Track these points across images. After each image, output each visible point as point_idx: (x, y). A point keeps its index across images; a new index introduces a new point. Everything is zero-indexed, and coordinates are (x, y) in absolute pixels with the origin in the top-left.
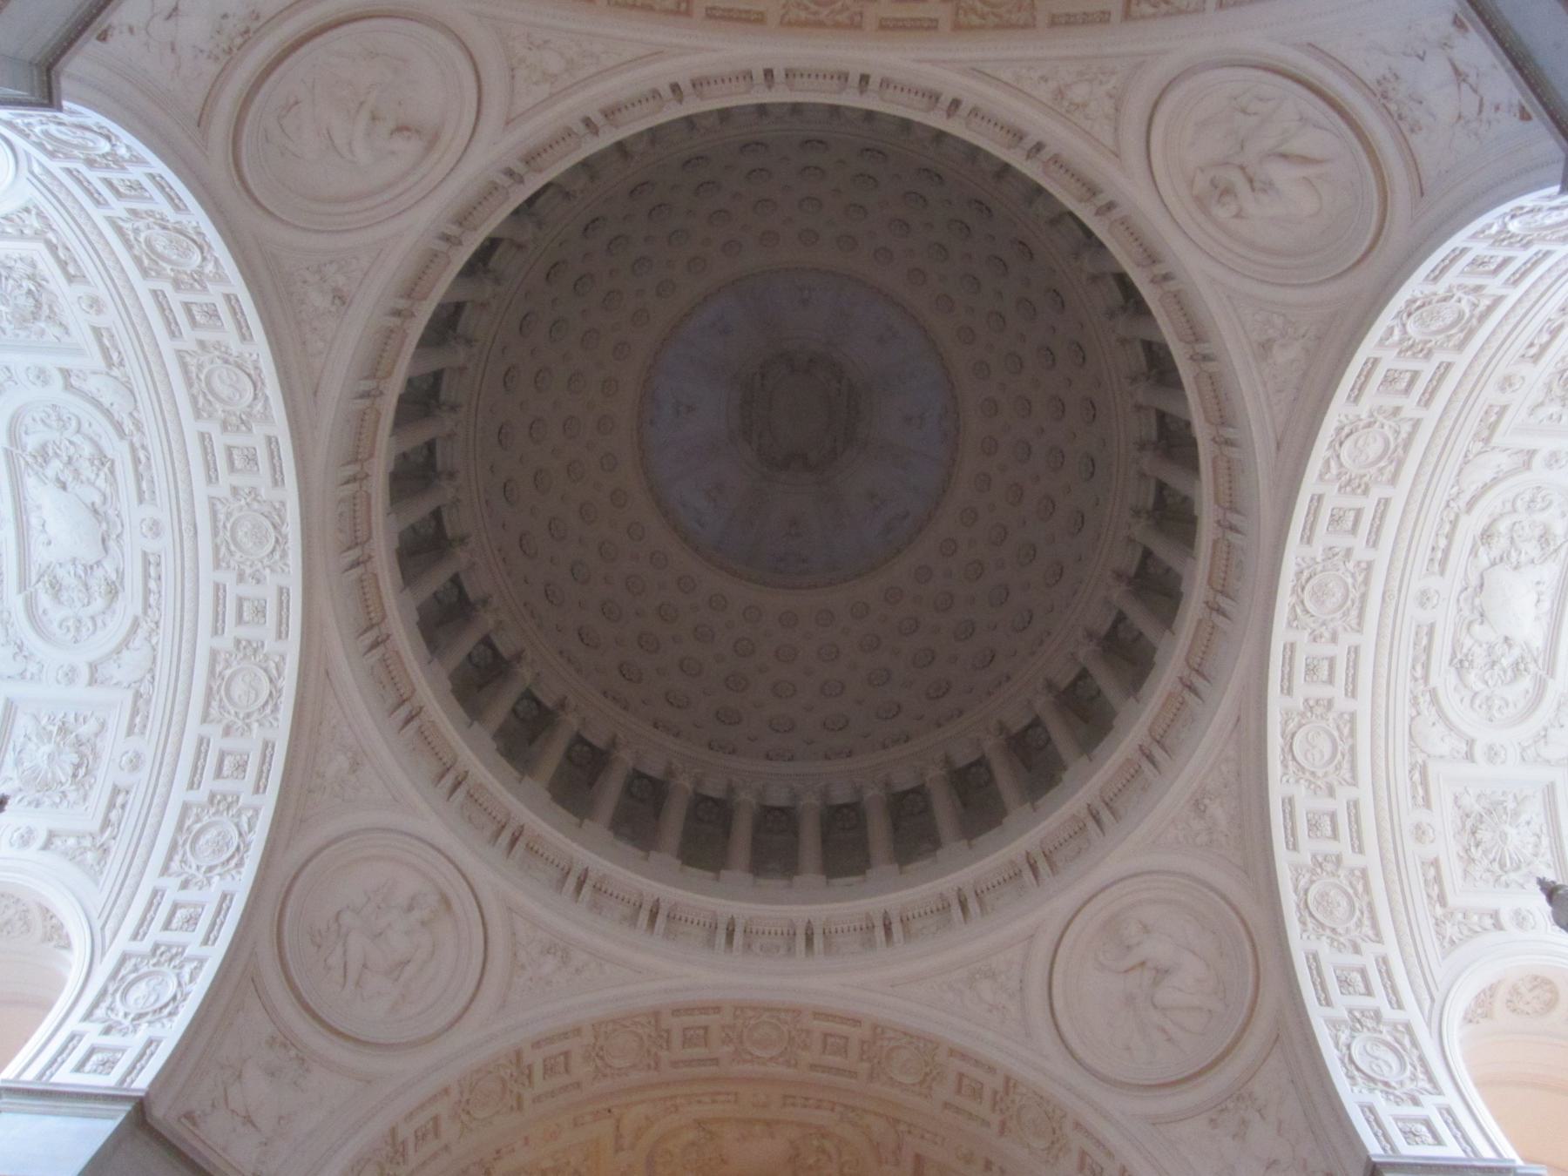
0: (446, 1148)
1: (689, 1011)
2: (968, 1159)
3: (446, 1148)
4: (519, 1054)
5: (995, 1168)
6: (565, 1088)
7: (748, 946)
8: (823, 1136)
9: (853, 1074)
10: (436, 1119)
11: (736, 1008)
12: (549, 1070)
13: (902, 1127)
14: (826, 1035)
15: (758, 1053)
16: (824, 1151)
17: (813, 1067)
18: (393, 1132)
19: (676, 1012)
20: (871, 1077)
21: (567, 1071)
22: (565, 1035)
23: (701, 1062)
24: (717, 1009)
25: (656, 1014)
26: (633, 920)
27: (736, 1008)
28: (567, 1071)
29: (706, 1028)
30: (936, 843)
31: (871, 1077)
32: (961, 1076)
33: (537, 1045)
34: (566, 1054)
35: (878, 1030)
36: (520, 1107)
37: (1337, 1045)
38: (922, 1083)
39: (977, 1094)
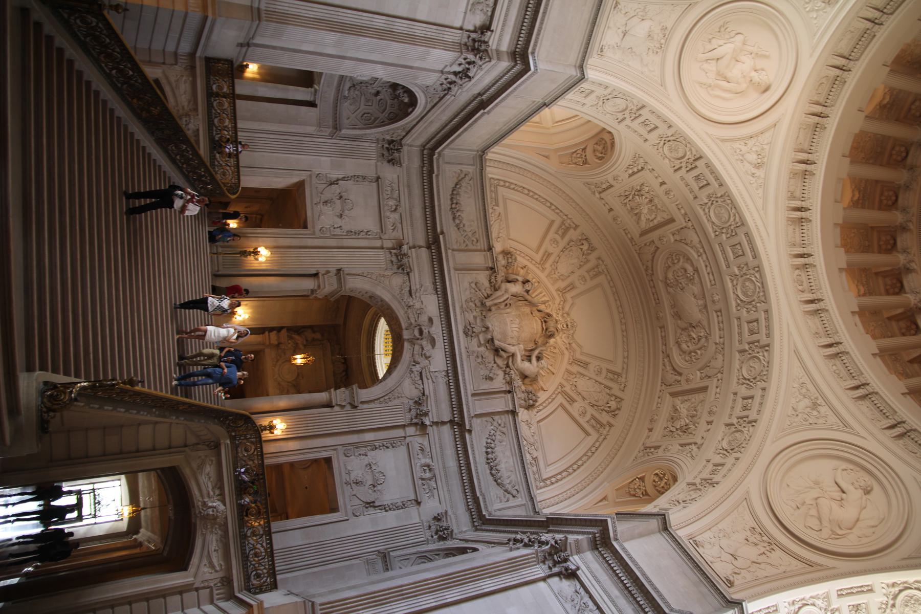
0: (646, 140)
1: (751, 242)
2: (711, 413)
3: (646, 140)
4: (701, 157)
5: (709, 426)
6: (692, 191)
7: (797, 268)
8: (706, 337)
9: (740, 342)
10: (656, 127)
11: (758, 267)
12: (697, 178)
13: (719, 375)
14: (757, 320)
15: (739, 288)
16: (699, 340)
17: (739, 319)
18: (643, 107)
19: (747, 235)
20: (742, 351)
21: (701, 188)
22: (717, 179)
23: (726, 259)
24: (755, 257)
25: (743, 224)
26: (792, 197)
27: (758, 267)
28: (701, 188)
29: (744, 255)
30: (874, 337)
31: (742, 351)
32: (752, 397)
33: (708, 165)
34: (708, 184)
35: (767, 347)
36: (675, 171)
37: (812, 597)
38: (745, 379)
39: (745, 408)
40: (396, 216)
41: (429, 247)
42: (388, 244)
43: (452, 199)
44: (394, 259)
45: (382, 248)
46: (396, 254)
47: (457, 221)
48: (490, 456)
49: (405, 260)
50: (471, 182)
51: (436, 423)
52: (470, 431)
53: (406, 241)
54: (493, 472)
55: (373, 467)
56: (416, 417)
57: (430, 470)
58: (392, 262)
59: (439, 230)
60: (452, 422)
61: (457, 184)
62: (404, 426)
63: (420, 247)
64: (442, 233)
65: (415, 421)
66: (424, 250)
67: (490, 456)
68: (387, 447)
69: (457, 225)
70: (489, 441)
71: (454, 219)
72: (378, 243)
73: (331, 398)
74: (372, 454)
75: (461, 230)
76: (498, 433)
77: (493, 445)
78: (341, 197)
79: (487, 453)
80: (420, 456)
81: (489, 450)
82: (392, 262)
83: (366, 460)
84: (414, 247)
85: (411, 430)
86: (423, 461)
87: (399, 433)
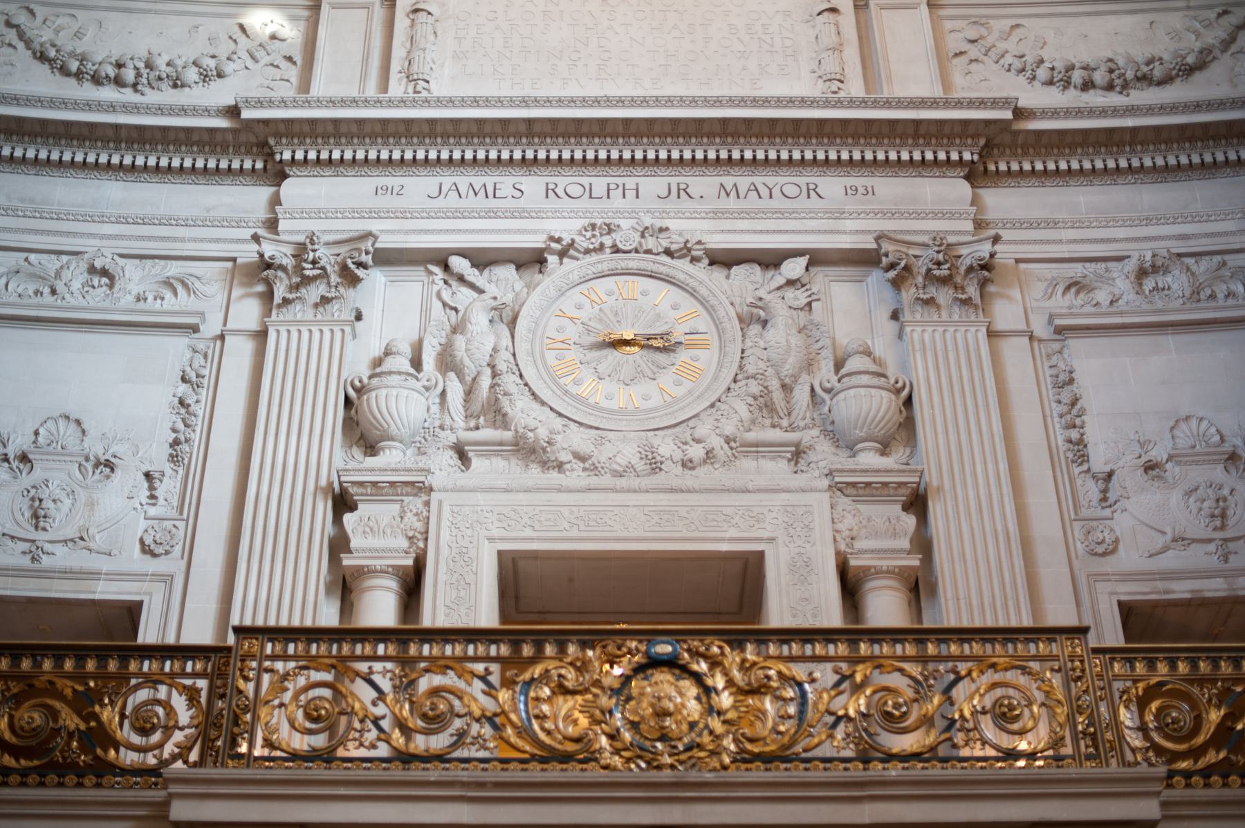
40: (134, 278)
41: (277, 174)
42: (247, 312)
43: (97, 80)
44: (314, 292)
45: (261, 335)
46: (295, 288)
47: (192, 75)
48: (1099, 77)
49: (325, 255)
50: (40, 11)
51: (979, 225)
52: (1019, 113)
53: (248, 253)
54: (1158, 73)
55: (1159, 453)
56: (958, 288)
57: (1155, 269)
58: (325, 300)
59: (222, 123)
60: (975, 175)
61: (42, 57)
62: (992, 334)
63: (276, 201)
64: (233, 112)
65: (972, 291)
66: (293, 189)
67: (1099, 77)
68: (1074, 403)
69: (205, 77)
70: (1042, 73)
71: (177, 83)
72: (239, 352)
73: (889, 572)
74: (1099, 459)
75: (229, 68)
76: (1011, 46)
77: (1059, 65)
78: (24, 458)
79: (1087, 85)
80: (1102, 296)
81: (1077, 76)
82: (325, 300)
83: (1129, 478)
84: (272, 224)
85: (1006, 313)
86: (1123, 285)
87: (1015, 352)
